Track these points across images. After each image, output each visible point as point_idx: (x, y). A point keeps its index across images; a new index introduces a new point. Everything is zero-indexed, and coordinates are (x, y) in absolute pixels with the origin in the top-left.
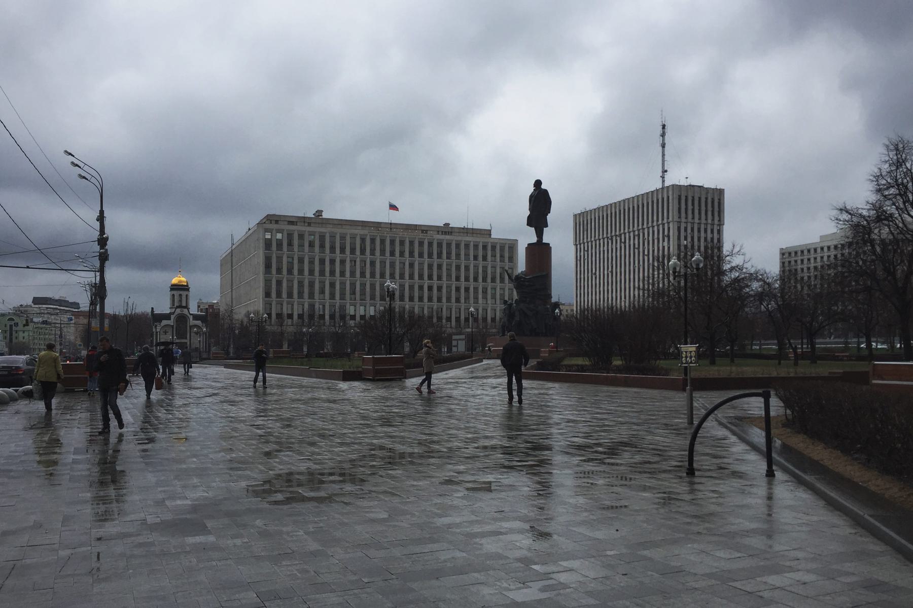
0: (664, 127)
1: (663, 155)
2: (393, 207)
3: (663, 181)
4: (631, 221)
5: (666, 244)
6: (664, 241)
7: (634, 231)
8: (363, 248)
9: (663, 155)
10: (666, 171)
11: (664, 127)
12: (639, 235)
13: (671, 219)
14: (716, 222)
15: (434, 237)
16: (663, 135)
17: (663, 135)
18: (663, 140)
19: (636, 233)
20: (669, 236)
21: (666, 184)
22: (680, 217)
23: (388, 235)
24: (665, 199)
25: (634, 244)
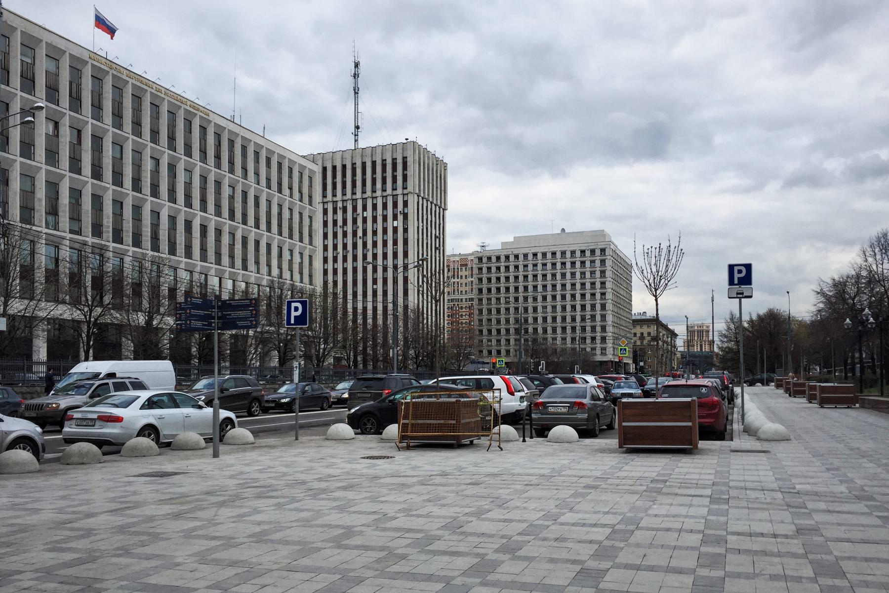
0: (357, 65)
2: (101, 23)
3: (356, 141)
5: (399, 223)
6: (395, 218)
7: (335, 202)
8: (74, 95)
11: (357, 65)
12: (345, 210)
13: (410, 188)
15: (211, 118)
16: (356, 76)
17: (356, 76)
18: (356, 83)
19: (340, 205)
20: (405, 216)
21: (362, 144)
23: (131, 81)
24: (399, 161)
25: (335, 222)
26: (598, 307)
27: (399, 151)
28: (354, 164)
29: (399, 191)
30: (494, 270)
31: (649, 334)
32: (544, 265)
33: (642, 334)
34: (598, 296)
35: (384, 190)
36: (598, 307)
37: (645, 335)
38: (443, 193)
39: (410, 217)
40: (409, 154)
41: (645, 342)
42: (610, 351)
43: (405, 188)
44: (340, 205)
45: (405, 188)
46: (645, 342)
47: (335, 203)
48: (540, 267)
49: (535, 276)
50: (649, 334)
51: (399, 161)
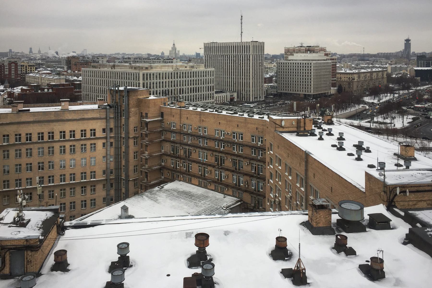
1: (241, 27)
4: (232, 51)
9: (241, 27)
10: (242, 32)
14: (263, 54)
19: (235, 56)
22: (253, 53)
24: (248, 46)
26: (309, 79)
27: (248, 43)
28: (238, 46)
29: (248, 54)
30: (285, 66)
31: (352, 77)
32: (296, 66)
33: (349, 77)
34: (309, 76)
35: (245, 53)
36: (309, 79)
37: (350, 78)
38: (263, 51)
39: (250, 60)
40: (250, 45)
41: (350, 80)
42: (312, 92)
43: (249, 53)
44: (235, 56)
45: (249, 53)
46: (350, 80)
47: (234, 55)
48: (294, 67)
49: (293, 69)
50: (352, 77)
51: (248, 46)
